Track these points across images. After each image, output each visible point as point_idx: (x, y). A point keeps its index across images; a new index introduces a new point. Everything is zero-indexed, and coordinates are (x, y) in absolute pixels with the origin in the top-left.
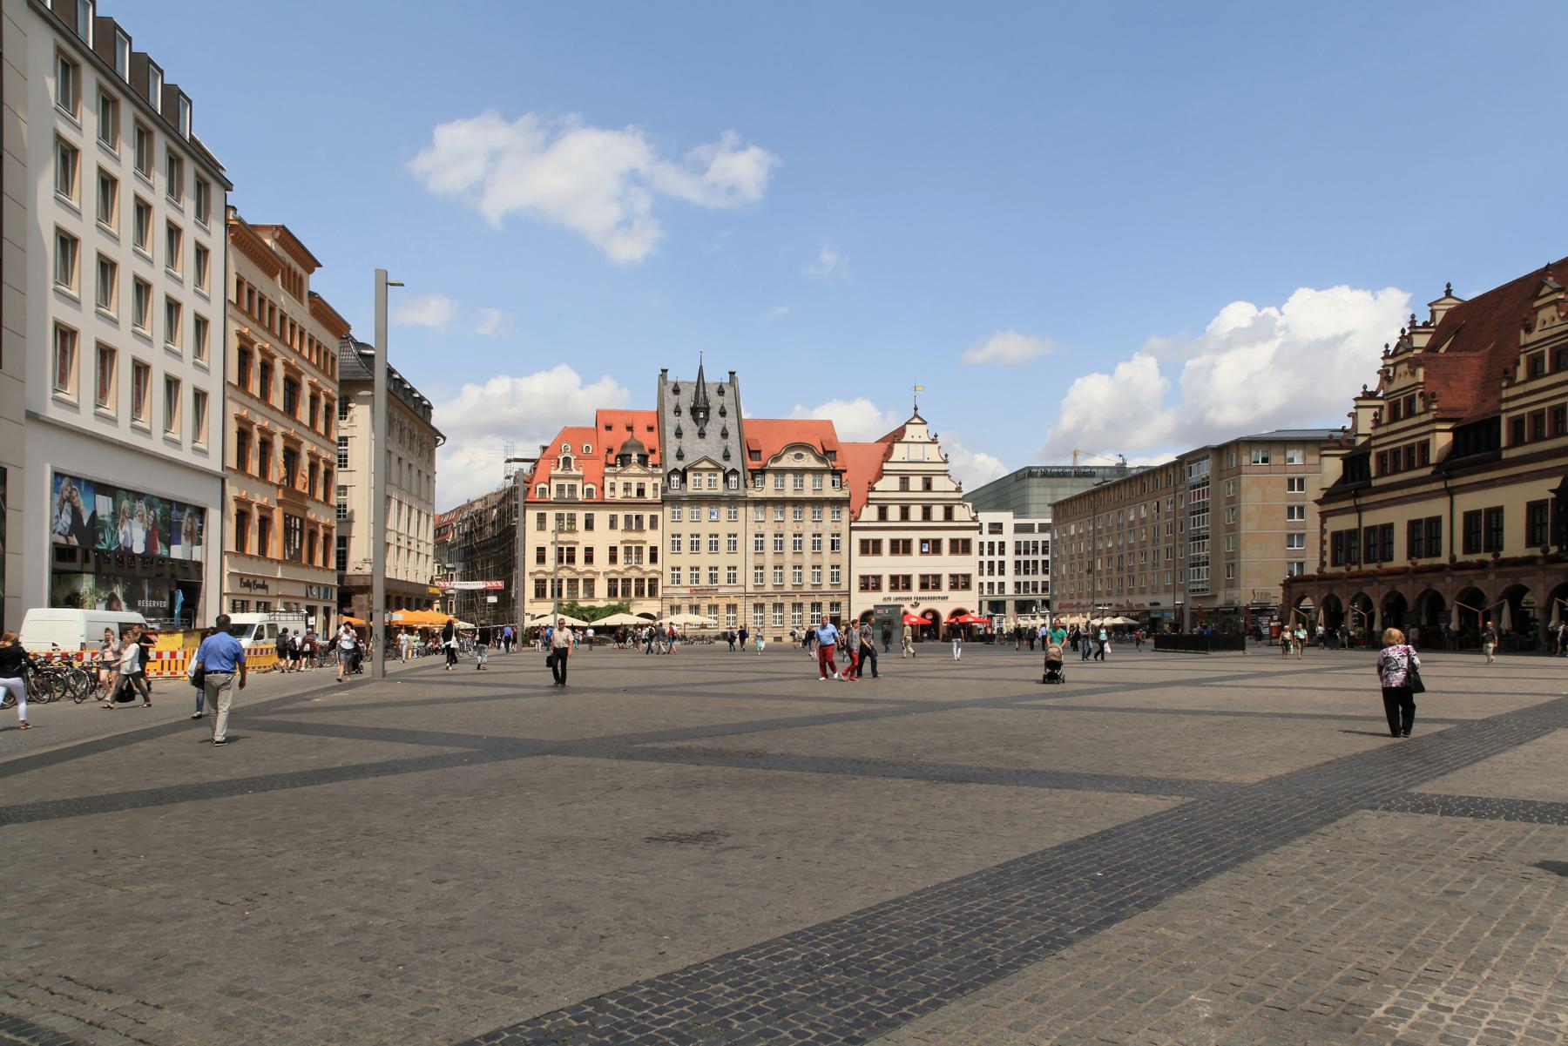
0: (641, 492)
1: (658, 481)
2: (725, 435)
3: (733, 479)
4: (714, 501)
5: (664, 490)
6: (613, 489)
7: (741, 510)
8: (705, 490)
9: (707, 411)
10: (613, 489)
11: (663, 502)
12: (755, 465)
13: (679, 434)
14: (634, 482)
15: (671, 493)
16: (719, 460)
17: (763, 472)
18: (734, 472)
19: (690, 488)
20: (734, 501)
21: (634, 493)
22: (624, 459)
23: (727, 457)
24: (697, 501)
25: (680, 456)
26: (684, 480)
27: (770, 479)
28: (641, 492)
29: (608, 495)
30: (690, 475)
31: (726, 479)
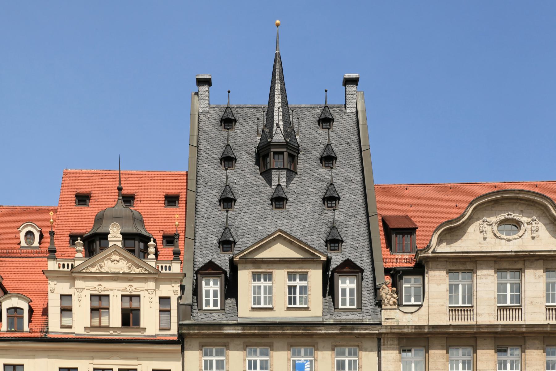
0: (130, 317)
1: (171, 290)
2: (331, 199)
3: (346, 285)
4: (300, 335)
5: (186, 310)
6: (66, 310)
7: (368, 359)
8: (281, 312)
9: (292, 152)
10: (66, 310)
11: (181, 340)
12: (402, 259)
13: (227, 202)
14: (115, 291)
15: (199, 318)
16: (317, 242)
17: (419, 269)
18: (350, 268)
19: (245, 309)
20: (348, 336)
21: (114, 318)
22: (94, 242)
23: (334, 242)
24: (263, 335)
25: (226, 244)
26: (231, 290)
27: (437, 281)
28: (130, 317)
29: (55, 325)
30: (244, 276)
31: (329, 288)
